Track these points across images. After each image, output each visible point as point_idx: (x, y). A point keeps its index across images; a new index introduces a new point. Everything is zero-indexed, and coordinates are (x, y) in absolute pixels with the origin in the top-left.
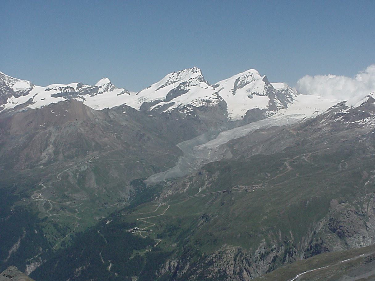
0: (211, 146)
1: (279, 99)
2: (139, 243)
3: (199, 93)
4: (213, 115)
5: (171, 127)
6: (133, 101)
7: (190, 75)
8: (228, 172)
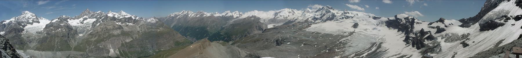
0: (231, 22)
1: (241, 15)
2: (222, 35)
3: (230, 14)
5: (226, 19)
6: (221, 15)
7: (229, 12)
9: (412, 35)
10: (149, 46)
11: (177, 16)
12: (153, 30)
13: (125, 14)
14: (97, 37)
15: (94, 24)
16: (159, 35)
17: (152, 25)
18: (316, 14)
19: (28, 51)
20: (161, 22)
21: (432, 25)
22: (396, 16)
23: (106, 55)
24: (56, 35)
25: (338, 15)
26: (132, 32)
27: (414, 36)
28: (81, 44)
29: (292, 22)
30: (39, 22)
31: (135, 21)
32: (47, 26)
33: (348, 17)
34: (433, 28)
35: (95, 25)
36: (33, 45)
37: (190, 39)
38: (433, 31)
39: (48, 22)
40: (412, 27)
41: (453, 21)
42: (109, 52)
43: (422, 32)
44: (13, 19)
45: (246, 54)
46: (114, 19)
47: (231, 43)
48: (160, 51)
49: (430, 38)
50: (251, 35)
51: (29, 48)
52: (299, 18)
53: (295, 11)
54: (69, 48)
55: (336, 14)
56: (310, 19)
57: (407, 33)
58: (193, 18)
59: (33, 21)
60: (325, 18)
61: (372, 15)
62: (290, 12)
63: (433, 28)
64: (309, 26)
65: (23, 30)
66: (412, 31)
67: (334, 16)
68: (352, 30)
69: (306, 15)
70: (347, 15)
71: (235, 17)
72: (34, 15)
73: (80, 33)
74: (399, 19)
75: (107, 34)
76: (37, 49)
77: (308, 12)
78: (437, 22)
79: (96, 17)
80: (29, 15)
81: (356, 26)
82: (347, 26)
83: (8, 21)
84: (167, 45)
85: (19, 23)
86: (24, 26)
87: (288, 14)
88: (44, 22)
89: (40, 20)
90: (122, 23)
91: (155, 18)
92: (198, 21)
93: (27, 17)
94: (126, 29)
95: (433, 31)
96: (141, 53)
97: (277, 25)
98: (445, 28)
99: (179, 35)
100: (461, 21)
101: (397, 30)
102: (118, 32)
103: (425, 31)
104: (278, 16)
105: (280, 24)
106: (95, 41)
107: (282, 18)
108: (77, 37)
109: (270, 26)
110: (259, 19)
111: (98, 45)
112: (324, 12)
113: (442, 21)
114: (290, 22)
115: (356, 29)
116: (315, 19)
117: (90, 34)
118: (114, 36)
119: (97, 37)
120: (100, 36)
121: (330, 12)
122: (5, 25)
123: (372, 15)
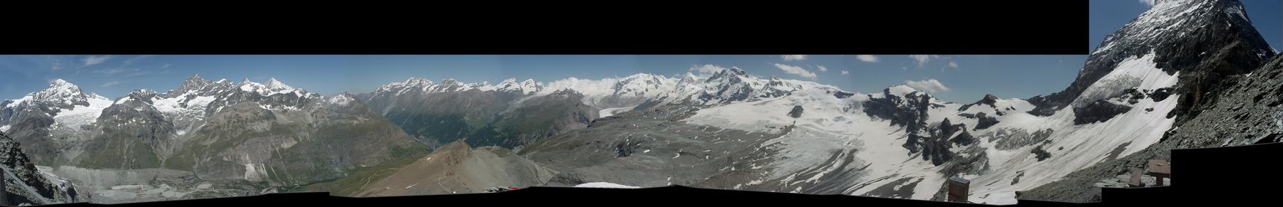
0: (518, 103)
2: (497, 134)
3: (515, 86)
4: (519, 93)
6: (495, 89)
8: (523, 111)
9: (922, 133)
10: (334, 157)
11: (397, 90)
12: (343, 122)
13: (279, 86)
14: (217, 138)
15: (210, 109)
16: (356, 134)
17: (340, 109)
18: (709, 85)
19: (62, 168)
20: (361, 105)
21: (969, 111)
22: (887, 91)
23: (237, 177)
24: (125, 134)
25: (757, 87)
26: (294, 126)
27: (927, 135)
28: (183, 152)
29: (655, 103)
30: (87, 104)
31: (302, 102)
32: (106, 113)
33: (779, 93)
34: (971, 116)
35: (213, 111)
36: (74, 154)
37: (425, 141)
38: (971, 124)
39: (108, 103)
40: (924, 116)
41: (1016, 102)
42: (244, 170)
43: (946, 127)
44: (28, 98)
45: (551, 176)
46: (255, 96)
47: (517, 150)
48: (359, 168)
49: (964, 139)
50: (563, 132)
51: (67, 162)
52: (671, 95)
53: (661, 80)
54: (153, 162)
55: (752, 86)
56: (694, 98)
57: (912, 129)
58: (432, 95)
59: (75, 102)
60: (728, 94)
61: (833, 88)
62: (648, 82)
63: (971, 116)
64: (692, 112)
65: (53, 121)
66: (922, 124)
67: (747, 89)
68: (789, 121)
69: (687, 89)
70: (778, 87)
71: (526, 91)
72: (76, 87)
73: (179, 128)
74: (893, 96)
75: (240, 131)
76: (84, 164)
77: (691, 81)
78: (979, 103)
79: (214, 94)
80: (64, 87)
81: (797, 112)
82: (777, 113)
83: (17, 102)
84: (374, 155)
85: (43, 107)
86: (54, 113)
87: (645, 85)
88: (98, 105)
89: (90, 100)
90: (273, 106)
91: (347, 95)
92: (443, 101)
93: (60, 93)
94: (282, 119)
95: (971, 124)
96: (316, 174)
97: (620, 110)
98: (998, 117)
99: (402, 133)
100: (1032, 101)
101: (888, 122)
102: (266, 125)
103: (953, 123)
104: (624, 90)
105: (626, 109)
106: (213, 146)
107: (632, 94)
108: (173, 137)
109: (605, 113)
110: (580, 96)
111: (220, 154)
112: (726, 81)
113: (989, 101)
114: (650, 103)
115: (797, 120)
116: (706, 96)
117: (203, 131)
118: (255, 134)
119: (217, 138)
120: (223, 135)
121: (738, 80)
122: (10, 110)
123: (833, 88)
